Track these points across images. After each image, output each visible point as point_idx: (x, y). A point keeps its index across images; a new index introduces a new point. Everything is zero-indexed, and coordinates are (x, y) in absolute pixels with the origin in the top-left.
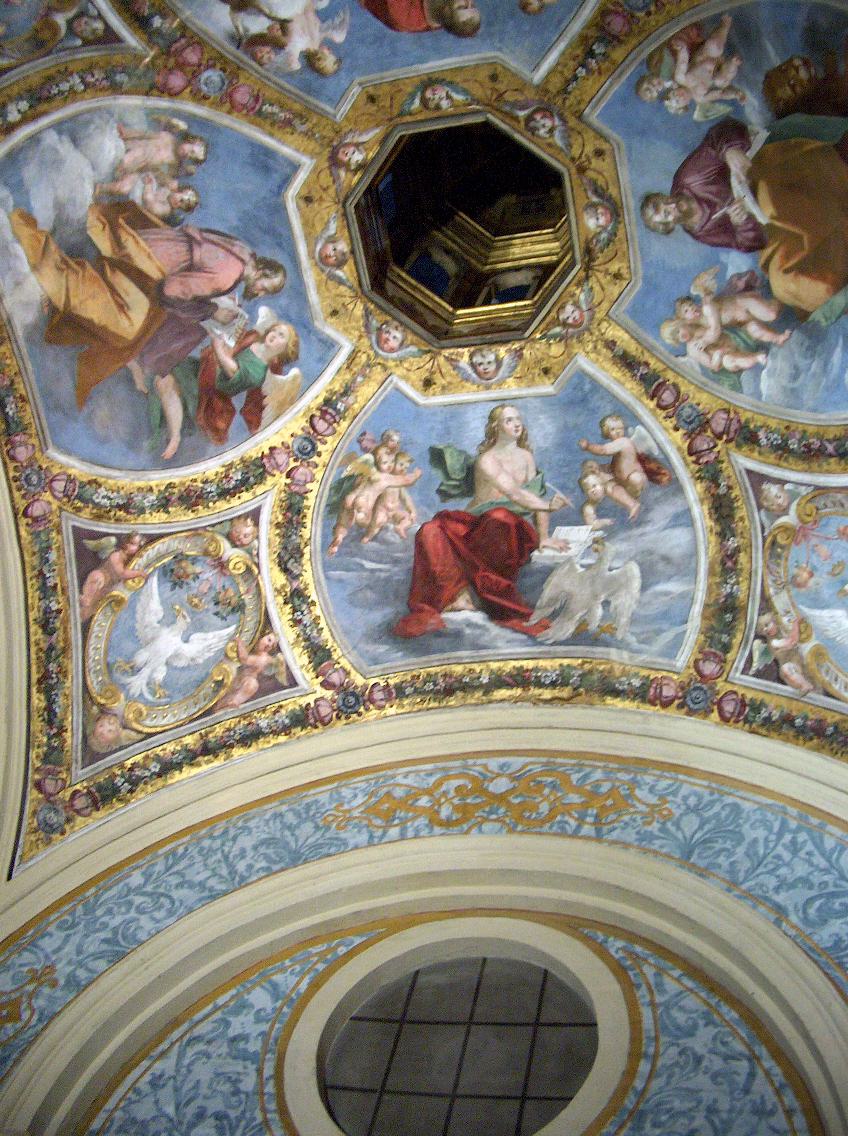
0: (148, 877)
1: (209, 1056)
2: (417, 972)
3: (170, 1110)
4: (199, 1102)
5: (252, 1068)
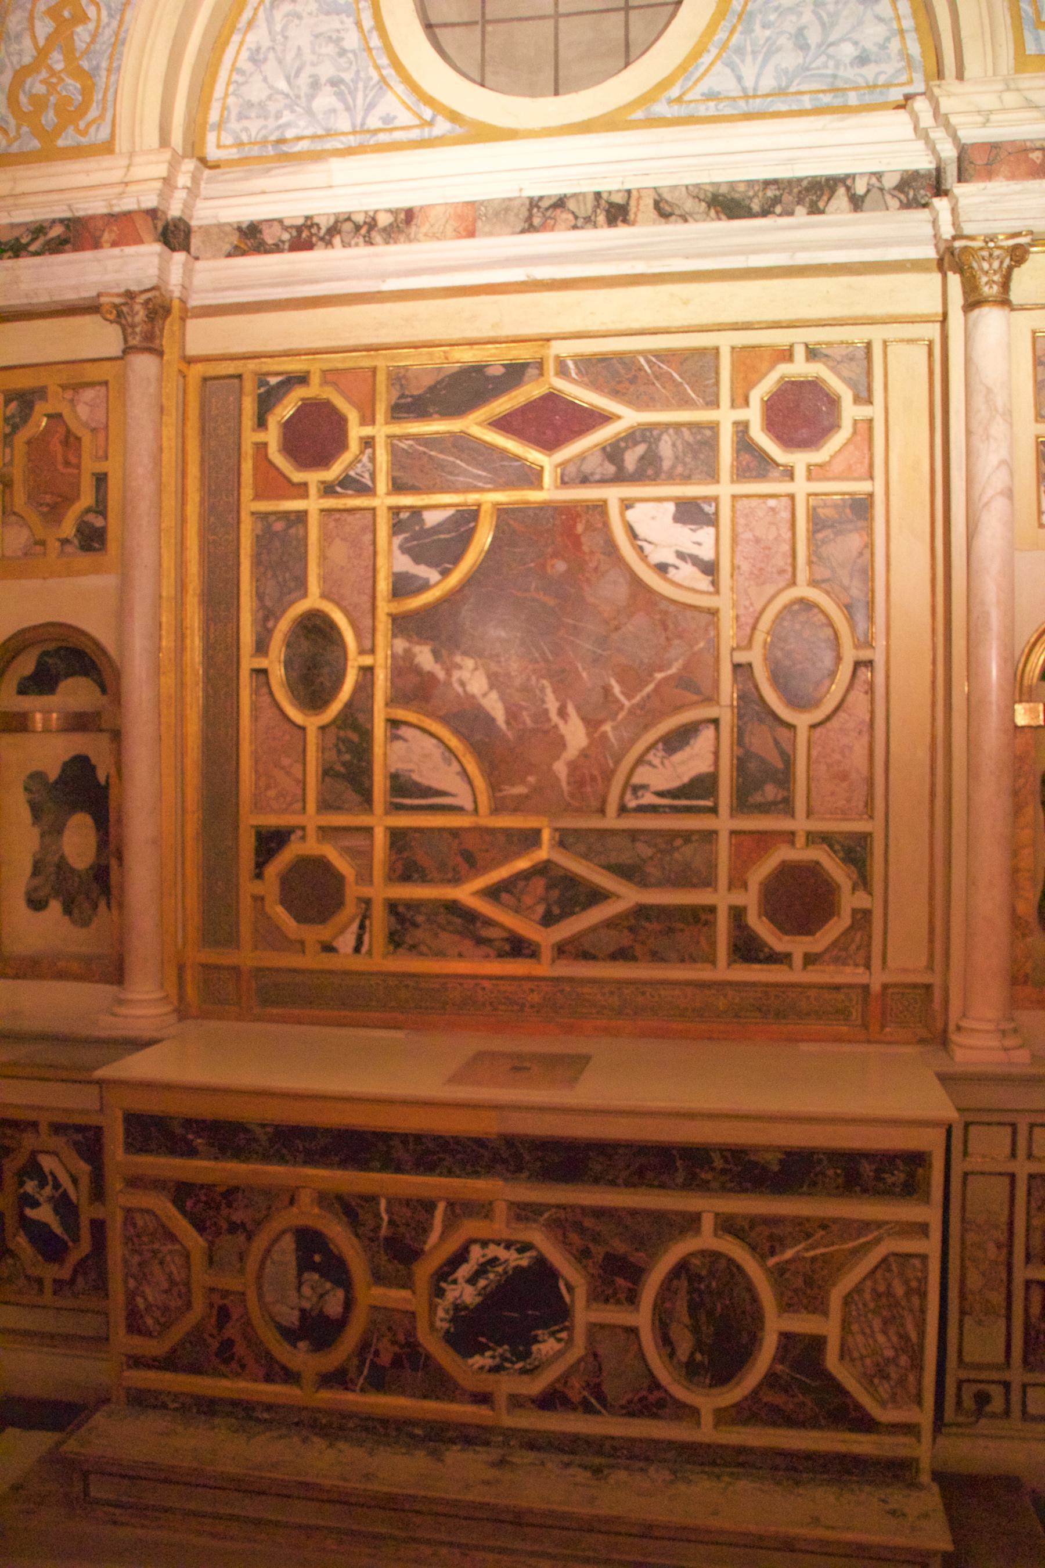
1: (299, 17)
3: (282, 85)
4: (308, 71)
5: (349, 22)
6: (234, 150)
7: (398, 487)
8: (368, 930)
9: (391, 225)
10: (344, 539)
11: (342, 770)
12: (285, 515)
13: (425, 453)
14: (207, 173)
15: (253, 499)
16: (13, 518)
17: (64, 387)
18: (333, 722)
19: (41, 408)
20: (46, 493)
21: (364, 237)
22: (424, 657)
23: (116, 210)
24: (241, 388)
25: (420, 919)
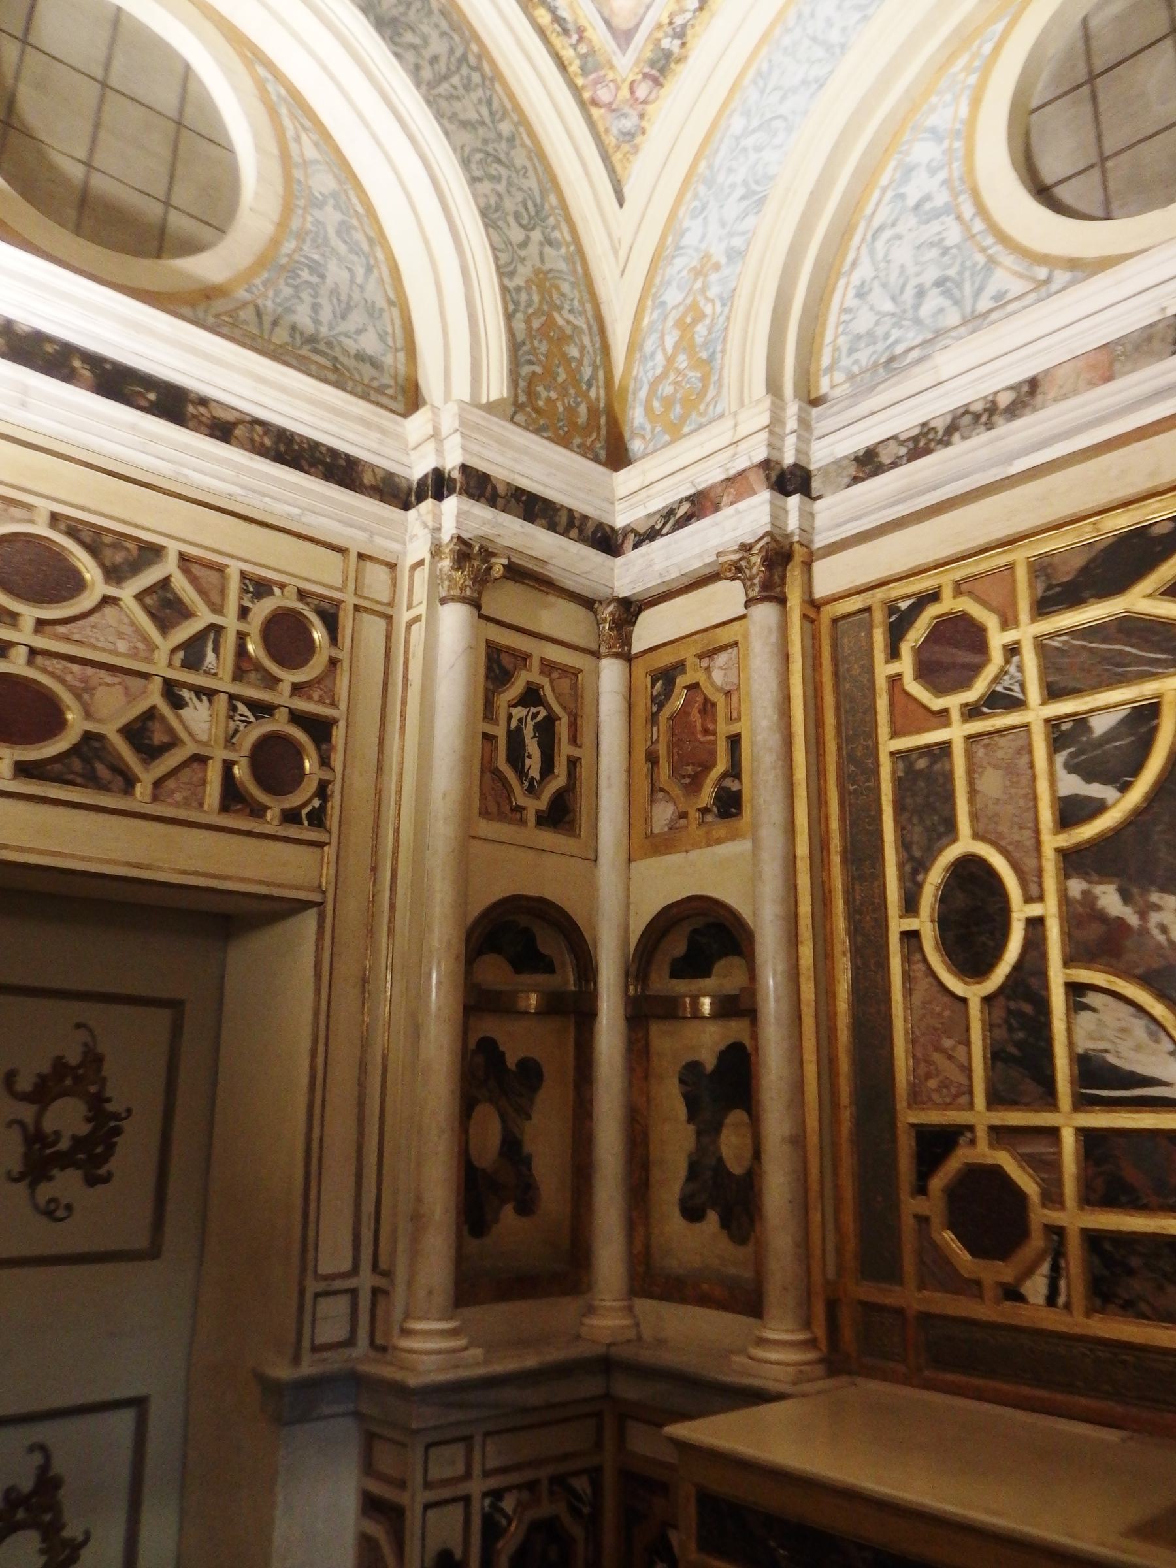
0: (747, 114)
2: (1085, 21)
3: (888, 306)
5: (949, 220)
6: (847, 385)
7: (1053, 693)
8: (1064, 1273)
9: (1014, 403)
10: (996, 767)
11: (1012, 1050)
12: (926, 750)
13: (1083, 647)
14: (815, 411)
15: (892, 738)
16: (661, 794)
17: (700, 657)
18: (1002, 989)
19: (682, 681)
20: (688, 765)
21: (986, 424)
22: (1109, 899)
23: (732, 472)
24: (871, 620)
25: (1135, 1262)
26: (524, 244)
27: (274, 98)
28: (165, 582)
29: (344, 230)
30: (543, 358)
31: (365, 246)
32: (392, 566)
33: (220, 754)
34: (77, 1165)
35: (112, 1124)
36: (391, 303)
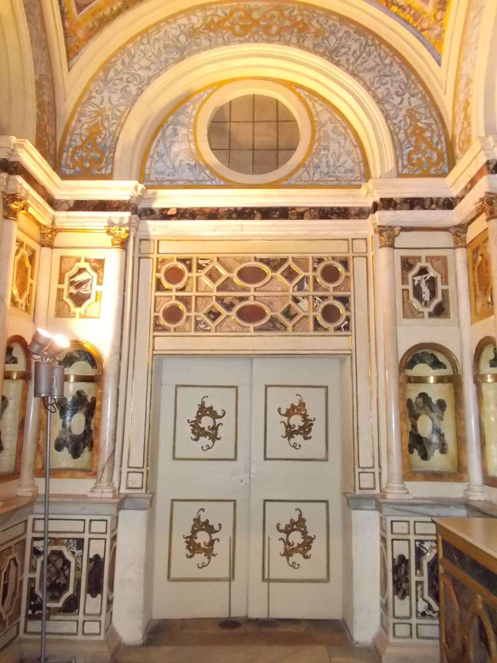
26: (401, 103)
27: (304, 97)
28: (289, 267)
29: (335, 130)
30: (413, 144)
31: (343, 131)
32: (366, 239)
33: (311, 314)
34: (301, 434)
35: (310, 422)
36: (355, 147)
